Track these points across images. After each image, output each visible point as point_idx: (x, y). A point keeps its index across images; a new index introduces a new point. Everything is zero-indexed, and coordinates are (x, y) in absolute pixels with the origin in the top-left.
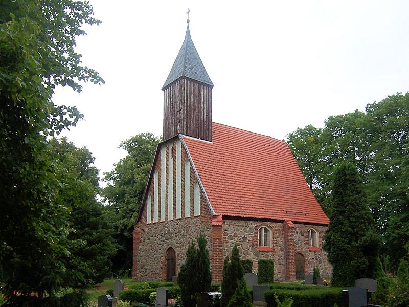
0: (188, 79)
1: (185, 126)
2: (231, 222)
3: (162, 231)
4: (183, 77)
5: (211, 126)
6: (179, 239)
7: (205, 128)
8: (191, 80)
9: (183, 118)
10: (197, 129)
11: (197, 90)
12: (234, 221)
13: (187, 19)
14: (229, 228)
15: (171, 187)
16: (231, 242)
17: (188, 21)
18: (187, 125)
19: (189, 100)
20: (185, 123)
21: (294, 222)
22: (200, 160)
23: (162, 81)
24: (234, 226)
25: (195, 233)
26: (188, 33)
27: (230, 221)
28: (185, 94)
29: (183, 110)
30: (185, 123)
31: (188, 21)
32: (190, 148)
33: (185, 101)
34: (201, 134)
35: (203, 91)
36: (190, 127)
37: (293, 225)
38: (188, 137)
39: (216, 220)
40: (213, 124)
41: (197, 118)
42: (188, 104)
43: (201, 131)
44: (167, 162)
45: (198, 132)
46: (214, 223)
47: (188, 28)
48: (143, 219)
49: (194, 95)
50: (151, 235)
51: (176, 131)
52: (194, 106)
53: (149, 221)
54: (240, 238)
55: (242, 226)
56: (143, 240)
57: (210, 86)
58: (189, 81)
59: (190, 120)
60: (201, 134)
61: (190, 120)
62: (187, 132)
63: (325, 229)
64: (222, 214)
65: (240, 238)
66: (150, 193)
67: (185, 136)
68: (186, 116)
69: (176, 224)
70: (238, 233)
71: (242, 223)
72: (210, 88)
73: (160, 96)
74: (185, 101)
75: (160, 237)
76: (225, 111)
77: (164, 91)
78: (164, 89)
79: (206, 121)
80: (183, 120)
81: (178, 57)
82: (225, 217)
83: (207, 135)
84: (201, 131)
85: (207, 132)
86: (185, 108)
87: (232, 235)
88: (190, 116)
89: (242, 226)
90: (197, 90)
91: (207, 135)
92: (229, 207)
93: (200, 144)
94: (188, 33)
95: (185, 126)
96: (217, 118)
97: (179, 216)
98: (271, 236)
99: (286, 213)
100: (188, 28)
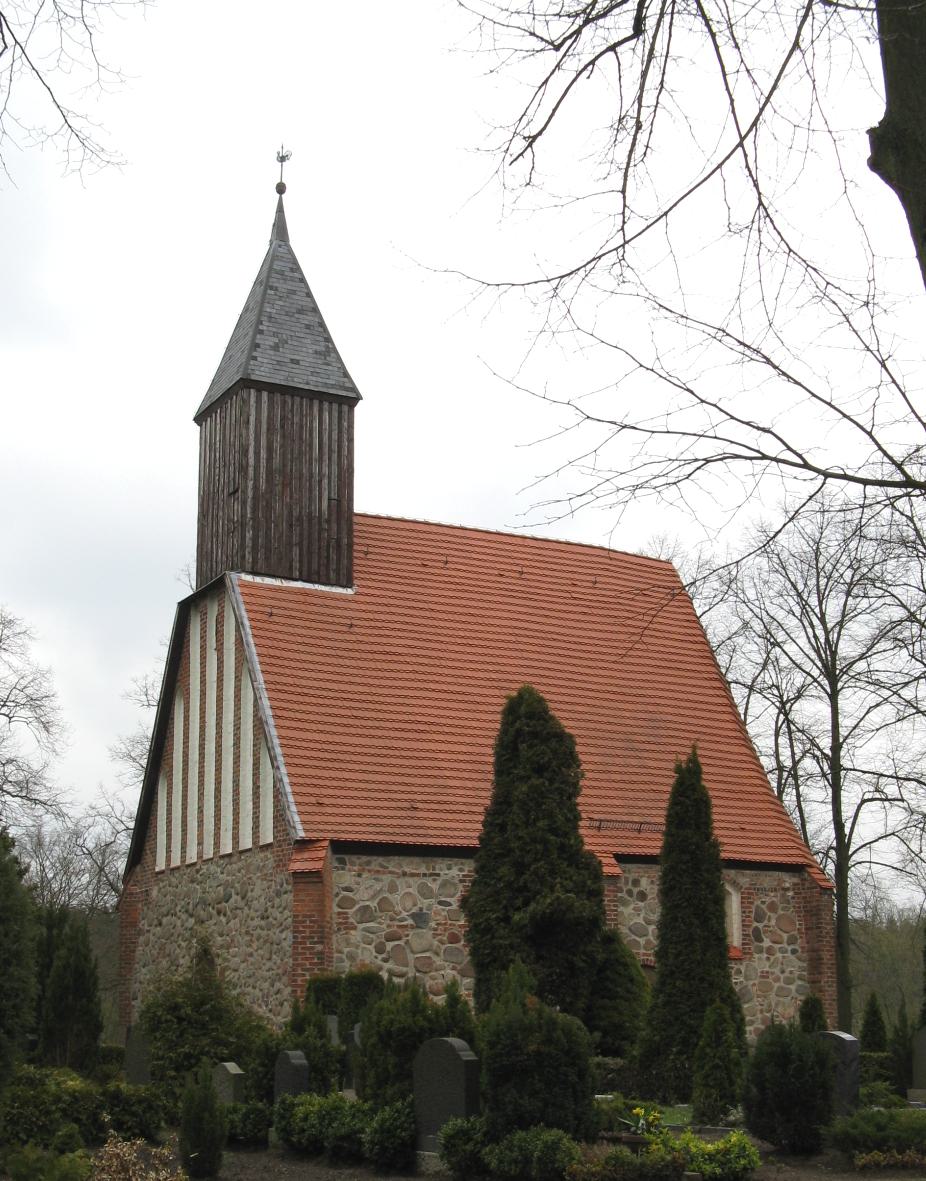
0: (260, 386)
1: (249, 542)
2: (368, 863)
3: (187, 895)
4: (246, 383)
5: (350, 531)
6: (223, 919)
7: (324, 544)
8: (273, 388)
9: (244, 516)
10: (296, 551)
11: (296, 420)
12: (381, 859)
13: (279, 181)
14: (359, 883)
15: (211, 747)
16: (365, 930)
17: (281, 189)
18: (255, 539)
19: (263, 454)
20: (249, 535)
21: (621, 859)
22: (442, 624)
23: (196, 396)
24: (380, 876)
25: (262, 900)
26: (280, 229)
27: (365, 859)
28: (252, 437)
29: (244, 492)
30: (249, 535)
31: (281, 189)
32: (258, 616)
33: (251, 461)
34: (310, 563)
35: (320, 420)
36: (268, 549)
37: (617, 870)
38: (258, 580)
39: (306, 855)
40: (355, 519)
41: (295, 513)
42: (263, 470)
43: (310, 553)
44: (203, 658)
45: (296, 558)
46: (297, 866)
47: (280, 210)
48: (148, 858)
49: (284, 437)
50: (164, 910)
51: (224, 558)
52: (282, 472)
53: (161, 865)
54: (404, 914)
55: (413, 875)
56: (146, 928)
57: (348, 400)
58: (265, 395)
59: (268, 520)
60: (310, 563)
61: (268, 520)
62: (255, 561)
63: (457, 873)
64: (331, 835)
65: (404, 914)
66: (164, 769)
67: (249, 578)
68: (255, 510)
69: (219, 870)
70: (395, 898)
71: (409, 865)
72: (345, 408)
73: (187, 443)
74: (251, 461)
75: (184, 916)
76: (390, 478)
77: (200, 425)
78: (199, 419)
79: (328, 521)
80: (243, 525)
81: (246, 309)
82: (343, 849)
83: (333, 566)
84: (310, 553)
85: (333, 556)
86: (250, 484)
87: (373, 904)
88: (269, 507)
89: (413, 875)
90: (296, 420)
91: (333, 566)
92: (432, 815)
93: (302, 598)
94: (280, 229)
95: (249, 542)
96: (370, 496)
97: (227, 848)
98: (734, 911)
99: (639, 831)
100: (280, 210)
